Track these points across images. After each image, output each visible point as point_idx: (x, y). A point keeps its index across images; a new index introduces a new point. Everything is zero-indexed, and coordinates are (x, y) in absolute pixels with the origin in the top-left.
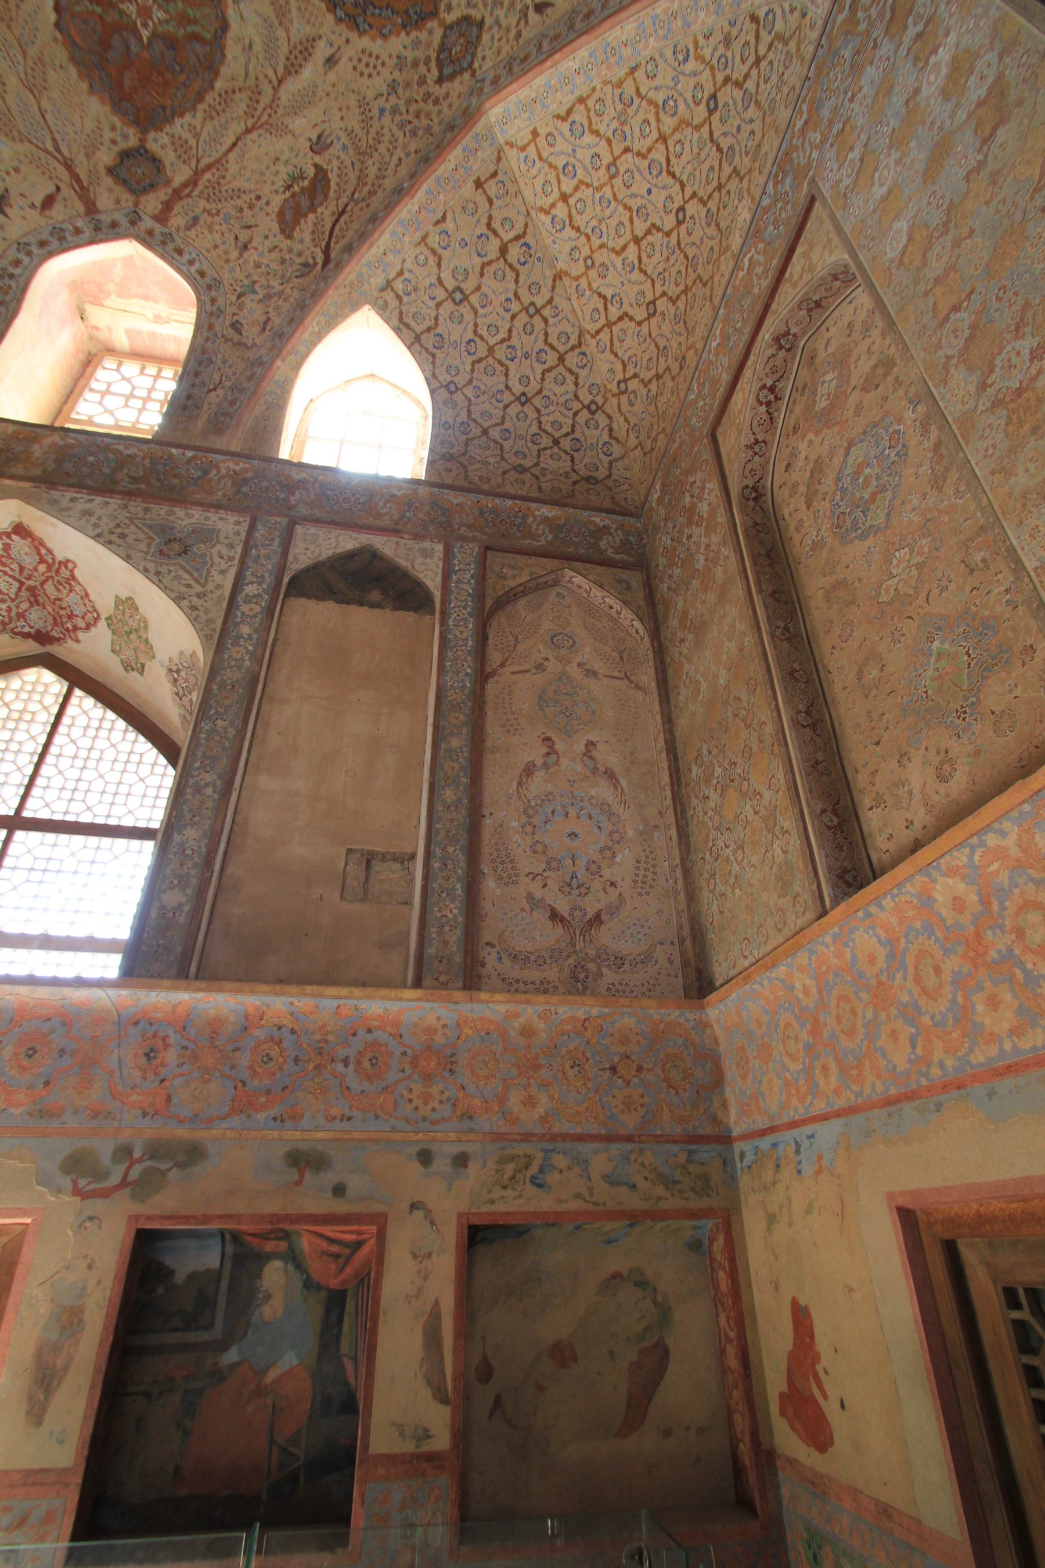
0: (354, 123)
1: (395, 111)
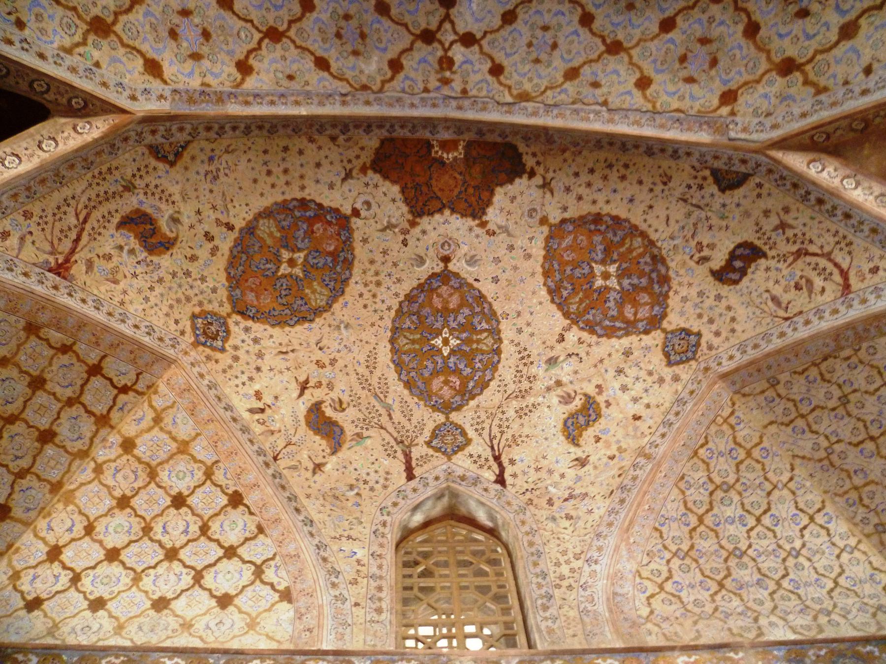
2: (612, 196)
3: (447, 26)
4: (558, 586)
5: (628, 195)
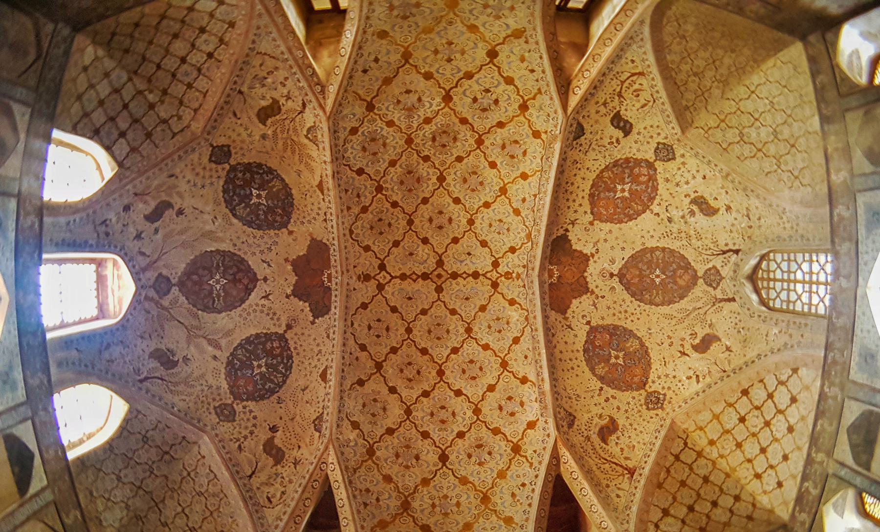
0: (197, 373)
1: (202, 390)
2: (581, 189)
3: (488, 275)
4: (797, 231)
5: (580, 180)
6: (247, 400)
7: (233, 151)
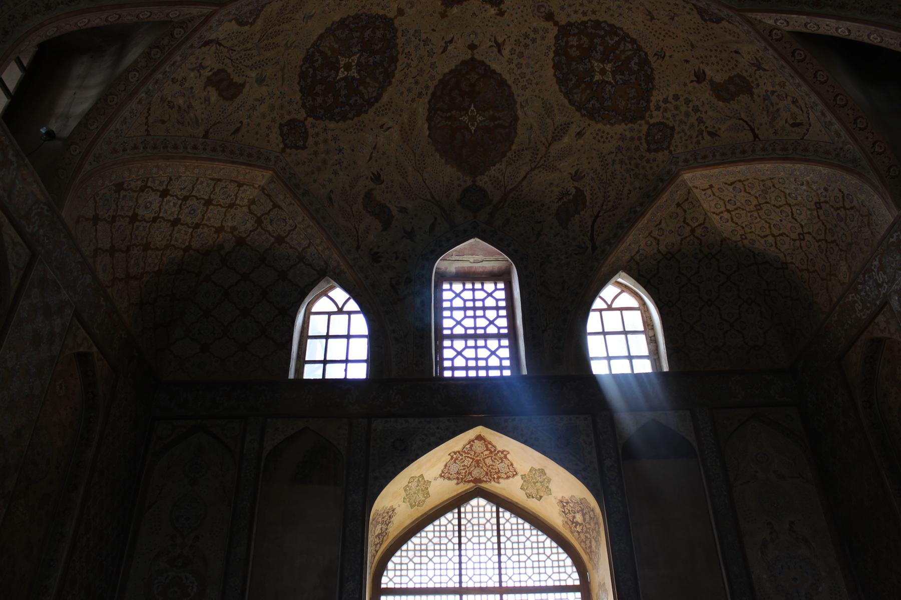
1: (621, 162)
6: (648, 101)
7: (287, 118)
